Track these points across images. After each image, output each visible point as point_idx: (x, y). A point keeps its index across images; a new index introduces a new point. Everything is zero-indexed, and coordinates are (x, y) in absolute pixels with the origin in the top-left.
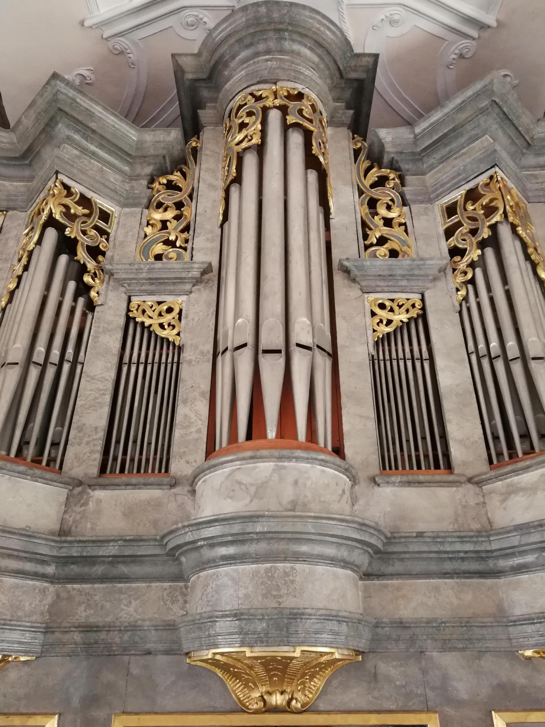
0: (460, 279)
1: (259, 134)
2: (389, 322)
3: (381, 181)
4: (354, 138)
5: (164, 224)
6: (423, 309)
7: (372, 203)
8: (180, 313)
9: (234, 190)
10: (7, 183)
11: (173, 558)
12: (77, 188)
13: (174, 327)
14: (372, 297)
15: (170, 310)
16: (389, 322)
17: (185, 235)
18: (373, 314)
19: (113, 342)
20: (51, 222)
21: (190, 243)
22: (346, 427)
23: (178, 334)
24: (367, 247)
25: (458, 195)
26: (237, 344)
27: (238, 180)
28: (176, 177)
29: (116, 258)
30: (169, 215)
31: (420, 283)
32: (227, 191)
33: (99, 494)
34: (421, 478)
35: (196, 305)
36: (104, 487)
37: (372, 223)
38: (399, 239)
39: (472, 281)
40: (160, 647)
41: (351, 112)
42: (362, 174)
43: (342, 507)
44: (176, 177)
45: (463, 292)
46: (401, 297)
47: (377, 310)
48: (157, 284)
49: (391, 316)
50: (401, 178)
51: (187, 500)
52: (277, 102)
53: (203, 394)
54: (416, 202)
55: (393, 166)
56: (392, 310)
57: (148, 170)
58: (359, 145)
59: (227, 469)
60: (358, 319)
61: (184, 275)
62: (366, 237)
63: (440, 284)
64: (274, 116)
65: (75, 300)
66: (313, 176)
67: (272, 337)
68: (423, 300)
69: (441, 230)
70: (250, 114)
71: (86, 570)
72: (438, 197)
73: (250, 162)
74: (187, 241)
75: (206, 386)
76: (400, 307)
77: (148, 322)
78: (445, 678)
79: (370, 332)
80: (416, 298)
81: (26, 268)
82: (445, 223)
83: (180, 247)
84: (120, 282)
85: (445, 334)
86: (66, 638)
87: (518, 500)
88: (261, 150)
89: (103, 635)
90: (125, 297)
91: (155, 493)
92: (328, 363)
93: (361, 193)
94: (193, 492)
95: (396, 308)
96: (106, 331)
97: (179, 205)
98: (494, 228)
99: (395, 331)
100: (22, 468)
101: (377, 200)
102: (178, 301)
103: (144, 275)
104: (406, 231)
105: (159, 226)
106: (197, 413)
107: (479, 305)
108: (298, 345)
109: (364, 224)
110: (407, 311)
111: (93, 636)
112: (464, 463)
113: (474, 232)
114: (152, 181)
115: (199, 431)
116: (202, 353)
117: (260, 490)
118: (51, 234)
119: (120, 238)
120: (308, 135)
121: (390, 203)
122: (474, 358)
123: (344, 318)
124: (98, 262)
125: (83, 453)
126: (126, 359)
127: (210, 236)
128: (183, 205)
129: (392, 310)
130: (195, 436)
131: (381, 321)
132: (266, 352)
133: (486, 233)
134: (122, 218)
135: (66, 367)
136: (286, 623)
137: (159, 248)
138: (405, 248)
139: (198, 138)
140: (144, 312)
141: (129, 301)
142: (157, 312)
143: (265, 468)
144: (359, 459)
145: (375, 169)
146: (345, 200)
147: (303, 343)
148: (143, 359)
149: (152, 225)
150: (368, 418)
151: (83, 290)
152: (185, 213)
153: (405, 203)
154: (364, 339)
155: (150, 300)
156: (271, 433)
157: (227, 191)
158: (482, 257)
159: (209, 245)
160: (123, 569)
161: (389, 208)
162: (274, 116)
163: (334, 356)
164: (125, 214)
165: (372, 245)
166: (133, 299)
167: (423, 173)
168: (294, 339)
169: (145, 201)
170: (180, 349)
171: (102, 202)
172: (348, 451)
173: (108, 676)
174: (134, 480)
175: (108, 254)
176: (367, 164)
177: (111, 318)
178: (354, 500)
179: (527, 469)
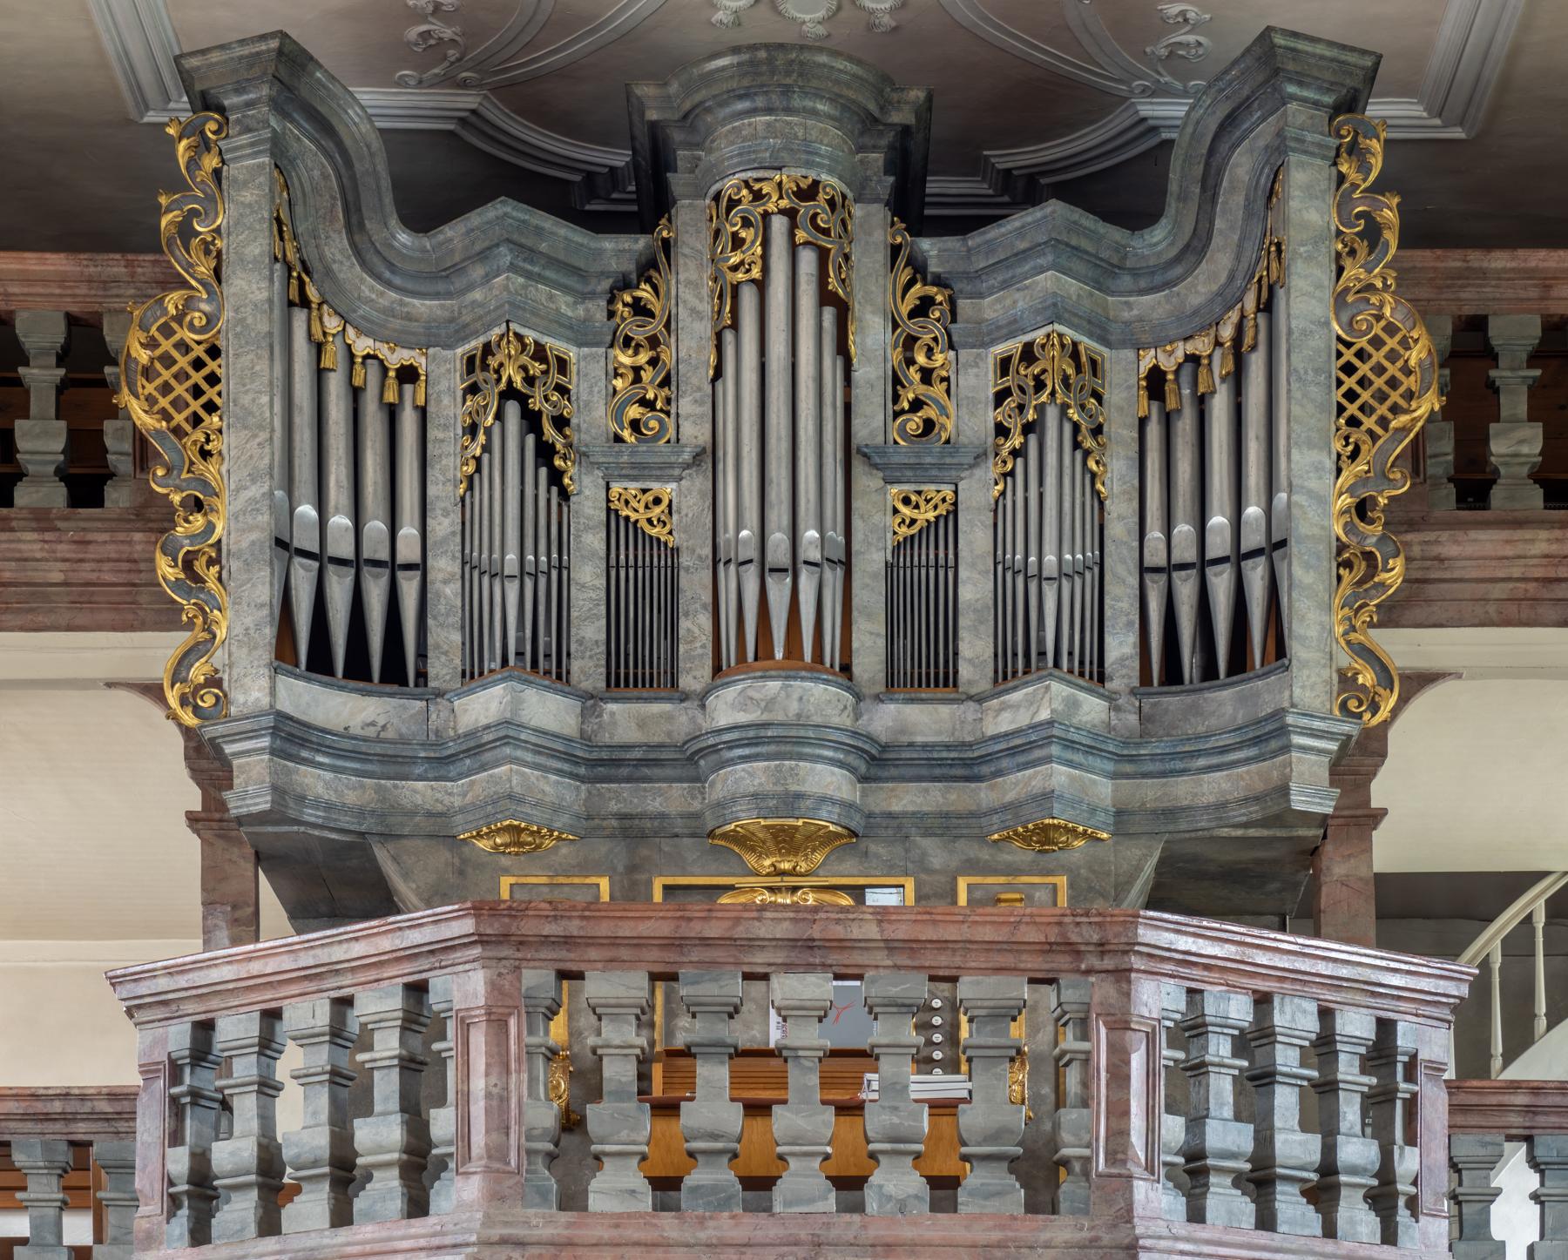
0: (1000, 470)
1: (760, 262)
2: (913, 522)
4: (893, 224)
5: (637, 370)
6: (955, 504)
7: (910, 342)
8: (670, 505)
9: (729, 336)
10: (416, 302)
12: (531, 336)
13: (665, 524)
14: (894, 489)
15: (657, 501)
16: (913, 522)
17: (665, 392)
18: (896, 511)
21: (673, 404)
22: (855, 645)
23: (670, 533)
24: (896, 415)
25: (1013, 346)
26: (741, 559)
27: (735, 326)
28: (645, 292)
29: (584, 426)
30: (643, 358)
31: (954, 473)
32: (719, 336)
33: (612, 707)
34: (923, 696)
35: (684, 493)
36: (615, 700)
37: (906, 377)
38: (936, 402)
39: (1012, 473)
40: (686, 831)
41: (891, 179)
42: (899, 294)
43: (846, 721)
45: (1000, 487)
46: (930, 489)
47: (900, 507)
48: (639, 471)
49: (914, 514)
50: (952, 302)
51: (698, 714)
52: (784, 203)
53: (704, 606)
54: (965, 346)
55: (939, 281)
56: (917, 507)
57: (606, 284)
58: (899, 240)
59: (739, 687)
60: (877, 518)
61: (673, 459)
62: (896, 398)
63: (978, 472)
64: (779, 224)
65: (549, 491)
66: (829, 314)
68: (956, 492)
69: (992, 391)
70: (746, 223)
71: (613, 771)
72: (993, 342)
73: (748, 298)
74: (668, 401)
75: (707, 597)
76: (928, 501)
77: (634, 516)
78: (924, 854)
79: (889, 535)
80: (947, 491)
81: (487, 448)
82: (996, 385)
83: (661, 410)
84: (599, 465)
85: (975, 538)
86: (605, 823)
87: (1006, 715)
88: (761, 285)
89: (637, 822)
90: (603, 483)
91: (667, 707)
92: (840, 572)
93: (895, 326)
94: (703, 707)
95: (922, 503)
96: (587, 528)
97: (654, 342)
98: (1040, 409)
99: (920, 531)
100: (547, 683)
101: (916, 339)
102: (668, 490)
103: (625, 458)
104: (948, 391)
105: (631, 377)
106: (700, 628)
107: (1014, 502)
108: (806, 562)
109: (896, 381)
110: (936, 507)
111: (627, 823)
112: (970, 682)
113: (1021, 408)
114: (611, 301)
115: (703, 646)
116: (700, 557)
117: (770, 704)
118: (512, 409)
119: (584, 397)
120: (823, 254)
121: (933, 344)
122: (1000, 568)
123: (862, 517)
124: (565, 437)
125: (588, 668)
126: (613, 562)
127: (698, 395)
128: (659, 344)
129: (917, 507)
130: (700, 651)
131: (903, 521)
132: (772, 570)
133: (1031, 415)
134: (582, 364)
135: (554, 574)
136: (791, 801)
137: (634, 412)
138: (943, 419)
139: (669, 220)
140: (627, 502)
141: (608, 489)
142: (642, 504)
143: (774, 686)
144: (866, 676)
145: (918, 286)
146: (873, 337)
147: (811, 559)
148: (631, 562)
149: (621, 375)
150: (878, 635)
151: (556, 477)
152: (663, 356)
153: (951, 347)
154: (881, 545)
155: (634, 488)
156: (779, 655)
157: (719, 336)
158: (1025, 445)
159: (698, 410)
160: (646, 771)
161: (930, 353)
162: (779, 224)
163: (847, 565)
164: (585, 358)
165: (903, 412)
166: (612, 485)
167: (981, 296)
168: (802, 556)
169: (609, 338)
170: (675, 551)
172: (856, 670)
173: (644, 852)
174: (645, 694)
175: (574, 421)
176: (905, 276)
177: (591, 512)
178: (857, 716)
179: (1015, 688)
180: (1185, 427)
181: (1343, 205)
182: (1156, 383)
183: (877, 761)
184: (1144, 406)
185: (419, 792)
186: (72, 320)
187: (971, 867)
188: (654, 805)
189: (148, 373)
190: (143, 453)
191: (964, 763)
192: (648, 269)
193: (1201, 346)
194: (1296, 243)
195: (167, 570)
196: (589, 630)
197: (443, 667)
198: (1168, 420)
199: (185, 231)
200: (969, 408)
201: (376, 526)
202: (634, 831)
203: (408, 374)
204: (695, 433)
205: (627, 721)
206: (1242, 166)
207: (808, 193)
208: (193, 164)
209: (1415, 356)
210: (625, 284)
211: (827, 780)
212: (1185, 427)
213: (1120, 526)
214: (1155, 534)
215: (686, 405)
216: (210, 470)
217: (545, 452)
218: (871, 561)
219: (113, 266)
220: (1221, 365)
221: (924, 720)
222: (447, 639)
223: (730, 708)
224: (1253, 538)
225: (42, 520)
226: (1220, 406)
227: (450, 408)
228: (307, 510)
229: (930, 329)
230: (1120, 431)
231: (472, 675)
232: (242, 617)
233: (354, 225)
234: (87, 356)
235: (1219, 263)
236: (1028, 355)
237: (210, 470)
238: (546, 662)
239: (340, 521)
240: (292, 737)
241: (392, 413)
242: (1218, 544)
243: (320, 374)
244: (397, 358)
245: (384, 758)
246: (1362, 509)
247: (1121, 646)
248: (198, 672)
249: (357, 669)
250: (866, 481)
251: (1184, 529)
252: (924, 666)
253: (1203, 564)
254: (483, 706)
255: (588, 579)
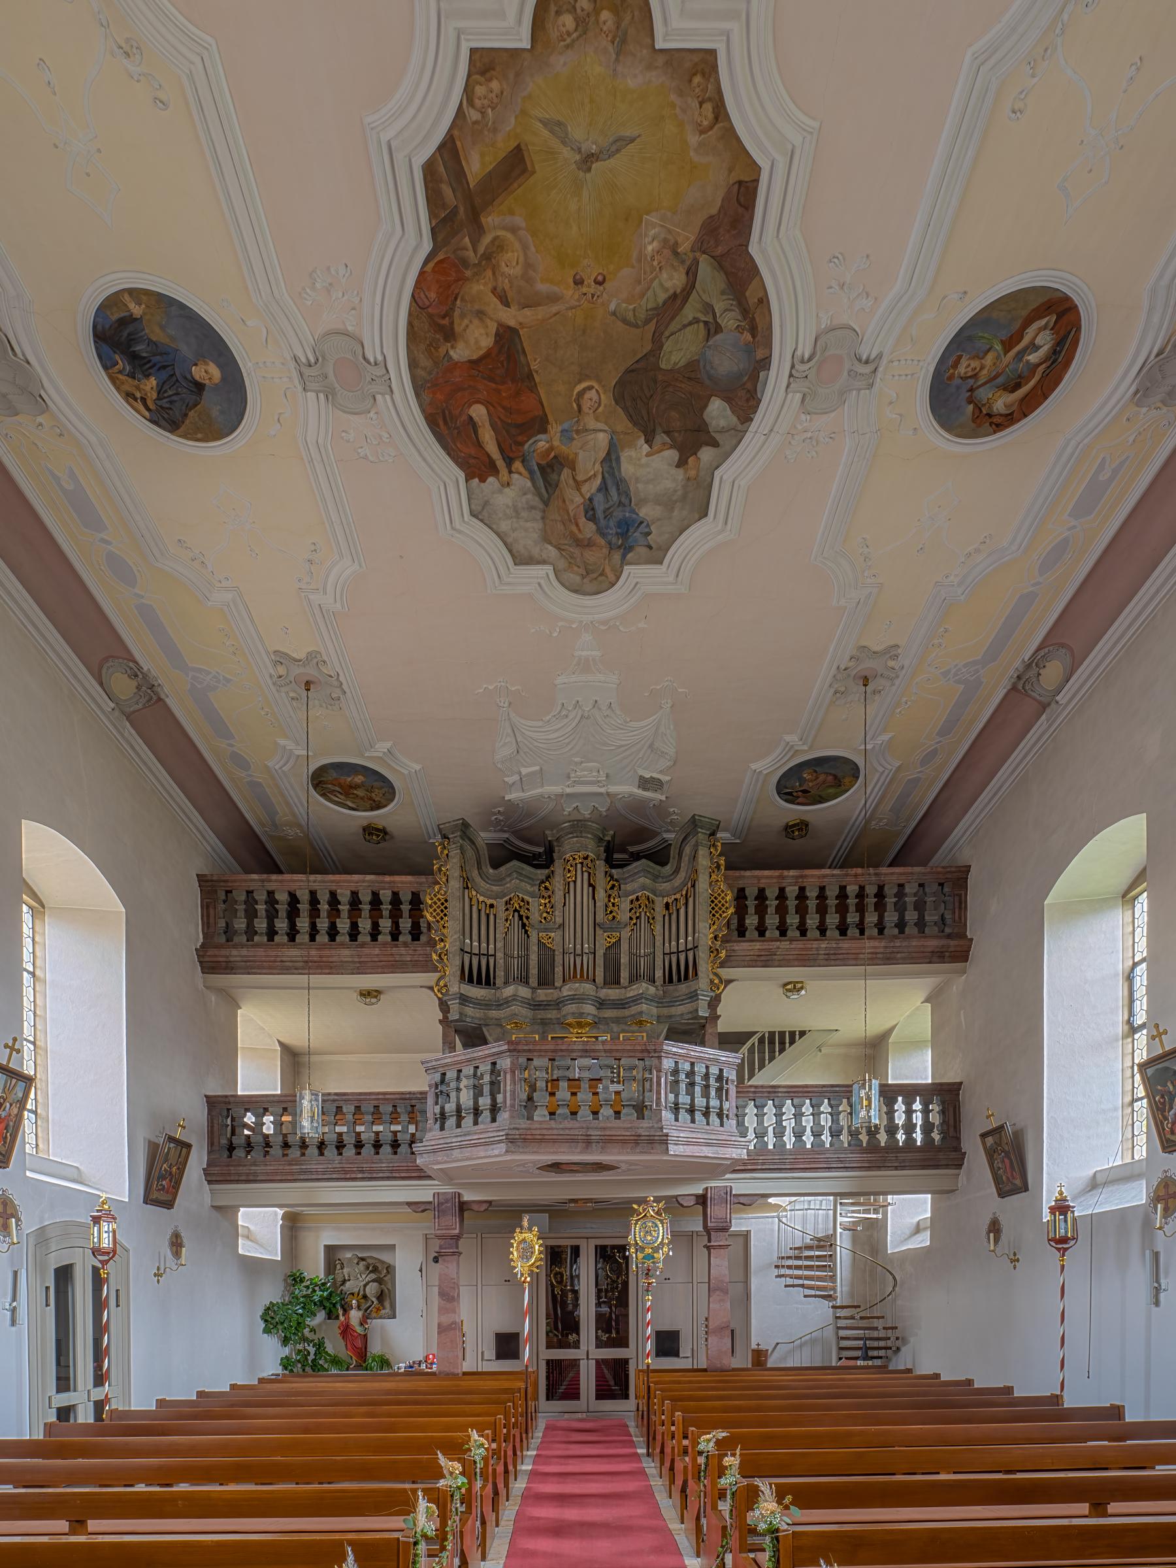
3: (613, 886)
11: (558, 1004)
19: (535, 948)
20: (516, 910)
25: (634, 897)
28: (547, 884)
44: (547, 884)
48: (546, 930)
67: (579, 951)
85: (625, 946)
117: (576, 990)
125: (533, 981)
136: (581, 1014)
146: (601, 894)
151: (526, 932)
171: (526, 897)
180: (674, 917)
181: (711, 859)
182: (667, 906)
183: (601, 1004)
184: (665, 912)
185: (494, 1013)
186: (413, 893)
187: (623, 1031)
188: (549, 1016)
189: (431, 906)
190: (429, 927)
191: (622, 1004)
192: (548, 877)
193: (678, 896)
194: (700, 869)
195: (435, 957)
196: (534, 971)
197: (499, 981)
198: (670, 915)
199: (440, 870)
200: (623, 916)
201: (484, 945)
202: (544, 1023)
203: (492, 906)
204: (559, 920)
205: (543, 994)
206: (688, 850)
207: (586, 858)
208: (442, 852)
209: (728, 898)
210: (543, 882)
211: (590, 1009)
212: (674, 917)
213: (659, 939)
214: (667, 945)
215: (557, 913)
216: (445, 931)
217: (524, 926)
218: (600, 953)
219: (423, 879)
220: (683, 901)
221: (612, 993)
222: (500, 974)
223: (566, 991)
224: (690, 946)
225: (405, 945)
226: (682, 911)
227: (502, 915)
228: (468, 941)
229: (614, 893)
230: (659, 918)
231: (506, 983)
232: (452, 969)
233: (479, 868)
234: (416, 901)
235: (682, 874)
236: (637, 899)
237: (445, 931)
238: (524, 980)
239: (476, 944)
240: (464, 999)
241: (488, 916)
242: (682, 948)
243: (471, 906)
244: (489, 902)
245: (486, 1005)
246: (716, 938)
247: (659, 974)
248: (442, 983)
249: (479, 982)
250: (599, 932)
251: (674, 943)
252: (613, 979)
253: (678, 952)
254: (509, 991)
255: (534, 957)
